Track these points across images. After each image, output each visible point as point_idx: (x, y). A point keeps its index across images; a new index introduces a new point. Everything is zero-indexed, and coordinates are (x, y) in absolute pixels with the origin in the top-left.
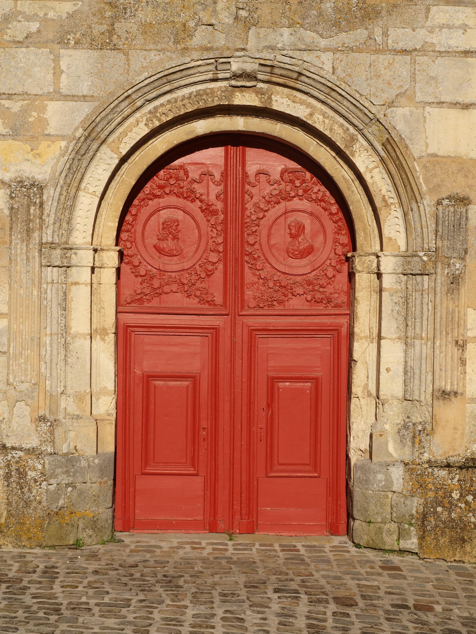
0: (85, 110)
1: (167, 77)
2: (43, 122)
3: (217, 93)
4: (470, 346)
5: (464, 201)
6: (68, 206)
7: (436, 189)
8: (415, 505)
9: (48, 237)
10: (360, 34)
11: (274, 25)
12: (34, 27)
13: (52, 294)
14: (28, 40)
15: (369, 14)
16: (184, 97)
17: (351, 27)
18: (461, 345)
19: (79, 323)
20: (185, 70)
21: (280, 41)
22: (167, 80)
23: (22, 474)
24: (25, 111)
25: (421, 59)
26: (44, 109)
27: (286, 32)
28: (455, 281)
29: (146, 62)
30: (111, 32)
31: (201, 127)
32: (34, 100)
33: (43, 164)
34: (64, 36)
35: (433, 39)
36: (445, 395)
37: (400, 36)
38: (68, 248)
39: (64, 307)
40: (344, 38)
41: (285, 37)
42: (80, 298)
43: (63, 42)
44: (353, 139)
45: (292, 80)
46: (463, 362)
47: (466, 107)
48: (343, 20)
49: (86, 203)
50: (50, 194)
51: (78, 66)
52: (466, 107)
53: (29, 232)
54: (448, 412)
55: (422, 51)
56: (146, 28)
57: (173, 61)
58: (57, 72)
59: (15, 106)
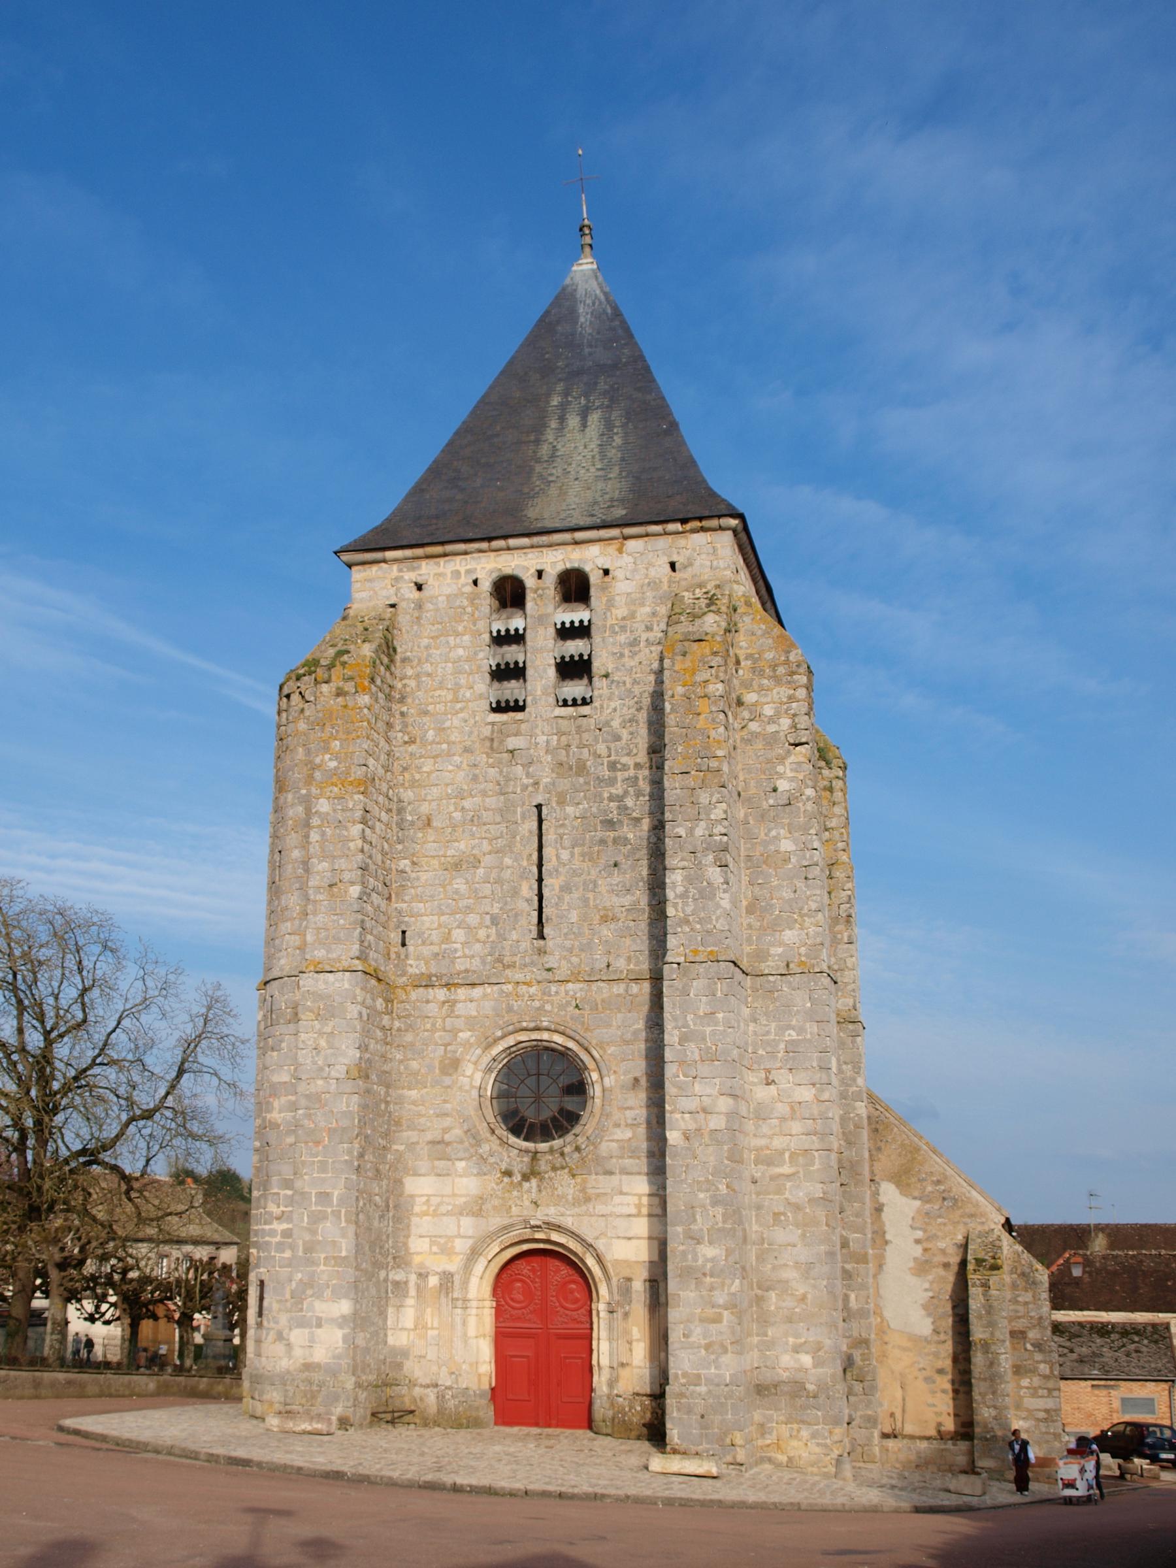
0: (470, 1242)
1: (505, 1228)
2: (453, 1247)
3: (527, 1233)
4: (634, 1344)
5: (629, 1280)
6: (465, 1283)
7: (617, 1274)
8: (610, 1413)
9: (455, 1296)
10: (584, 1208)
11: (548, 1205)
12: (450, 1208)
13: (458, 1320)
14: (448, 1214)
15: (588, 1200)
16: (514, 1235)
17: (580, 1206)
18: (630, 1343)
19: (472, 1331)
20: (512, 1225)
21: (550, 1212)
22: (506, 1228)
23: (443, 1397)
24: (446, 1243)
25: (610, 1218)
26: (453, 1242)
27: (552, 1208)
28: (626, 1315)
29: (496, 1222)
30: (481, 1209)
31: (525, 1247)
32: (451, 1238)
33: (453, 1265)
34: (460, 1212)
35: (615, 1210)
36: (623, 1365)
37: (601, 1208)
38: (465, 1300)
39: (464, 1323)
40: (577, 1210)
41: (552, 1210)
42: (472, 1322)
43: (461, 1214)
44: (584, 1253)
45: (558, 1228)
46: (631, 1350)
47: (630, 1239)
48: (576, 1202)
49: (474, 1281)
50: (457, 1278)
51: (467, 1223)
52: (630, 1239)
53: (447, 1293)
54: (624, 1373)
55: (611, 1215)
56: (494, 1207)
57: (506, 1221)
58: (459, 1226)
59: (442, 1241)
